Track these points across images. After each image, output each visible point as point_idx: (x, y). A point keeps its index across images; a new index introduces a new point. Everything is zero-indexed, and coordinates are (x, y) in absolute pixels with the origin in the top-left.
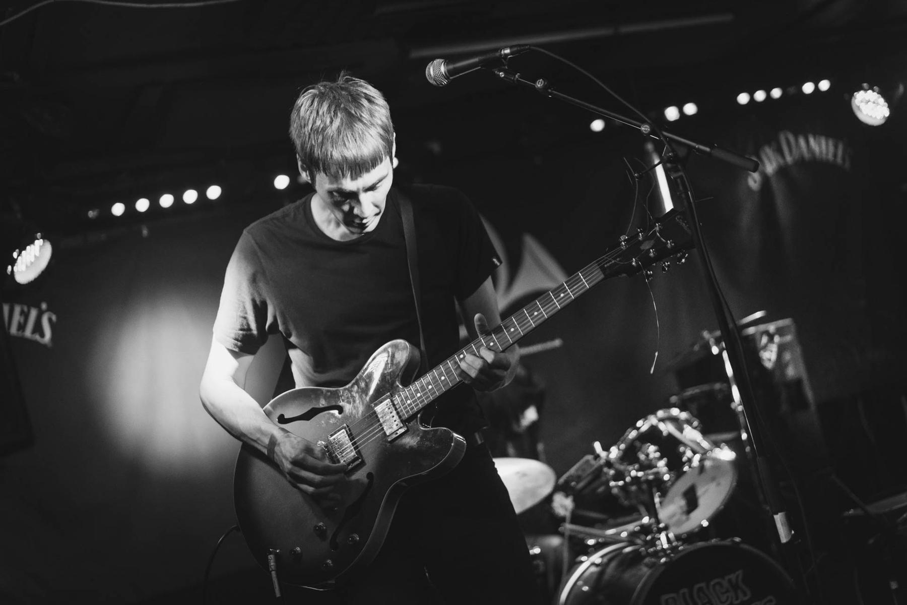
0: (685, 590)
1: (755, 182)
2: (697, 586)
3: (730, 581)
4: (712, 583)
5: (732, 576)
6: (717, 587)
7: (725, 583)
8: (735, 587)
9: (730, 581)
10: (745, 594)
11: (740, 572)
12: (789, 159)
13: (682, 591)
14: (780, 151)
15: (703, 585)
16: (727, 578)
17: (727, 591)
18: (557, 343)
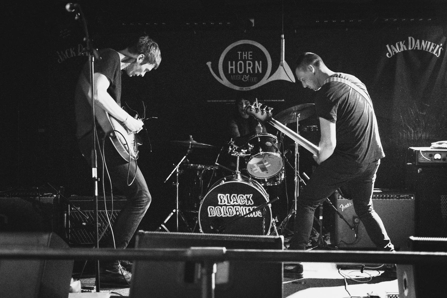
0: (229, 195)
1: (389, 55)
2: (233, 195)
3: (247, 197)
4: (239, 195)
5: (248, 196)
6: (241, 197)
7: (245, 197)
8: (248, 199)
9: (247, 197)
10: (251, 203)
11: (252, 195)
12: (410, 49)
13: (227, 195)
14: (406, 44)
15: (236, 195)
16: (246, 195)
17: (245, 200)
18: (283, 100)
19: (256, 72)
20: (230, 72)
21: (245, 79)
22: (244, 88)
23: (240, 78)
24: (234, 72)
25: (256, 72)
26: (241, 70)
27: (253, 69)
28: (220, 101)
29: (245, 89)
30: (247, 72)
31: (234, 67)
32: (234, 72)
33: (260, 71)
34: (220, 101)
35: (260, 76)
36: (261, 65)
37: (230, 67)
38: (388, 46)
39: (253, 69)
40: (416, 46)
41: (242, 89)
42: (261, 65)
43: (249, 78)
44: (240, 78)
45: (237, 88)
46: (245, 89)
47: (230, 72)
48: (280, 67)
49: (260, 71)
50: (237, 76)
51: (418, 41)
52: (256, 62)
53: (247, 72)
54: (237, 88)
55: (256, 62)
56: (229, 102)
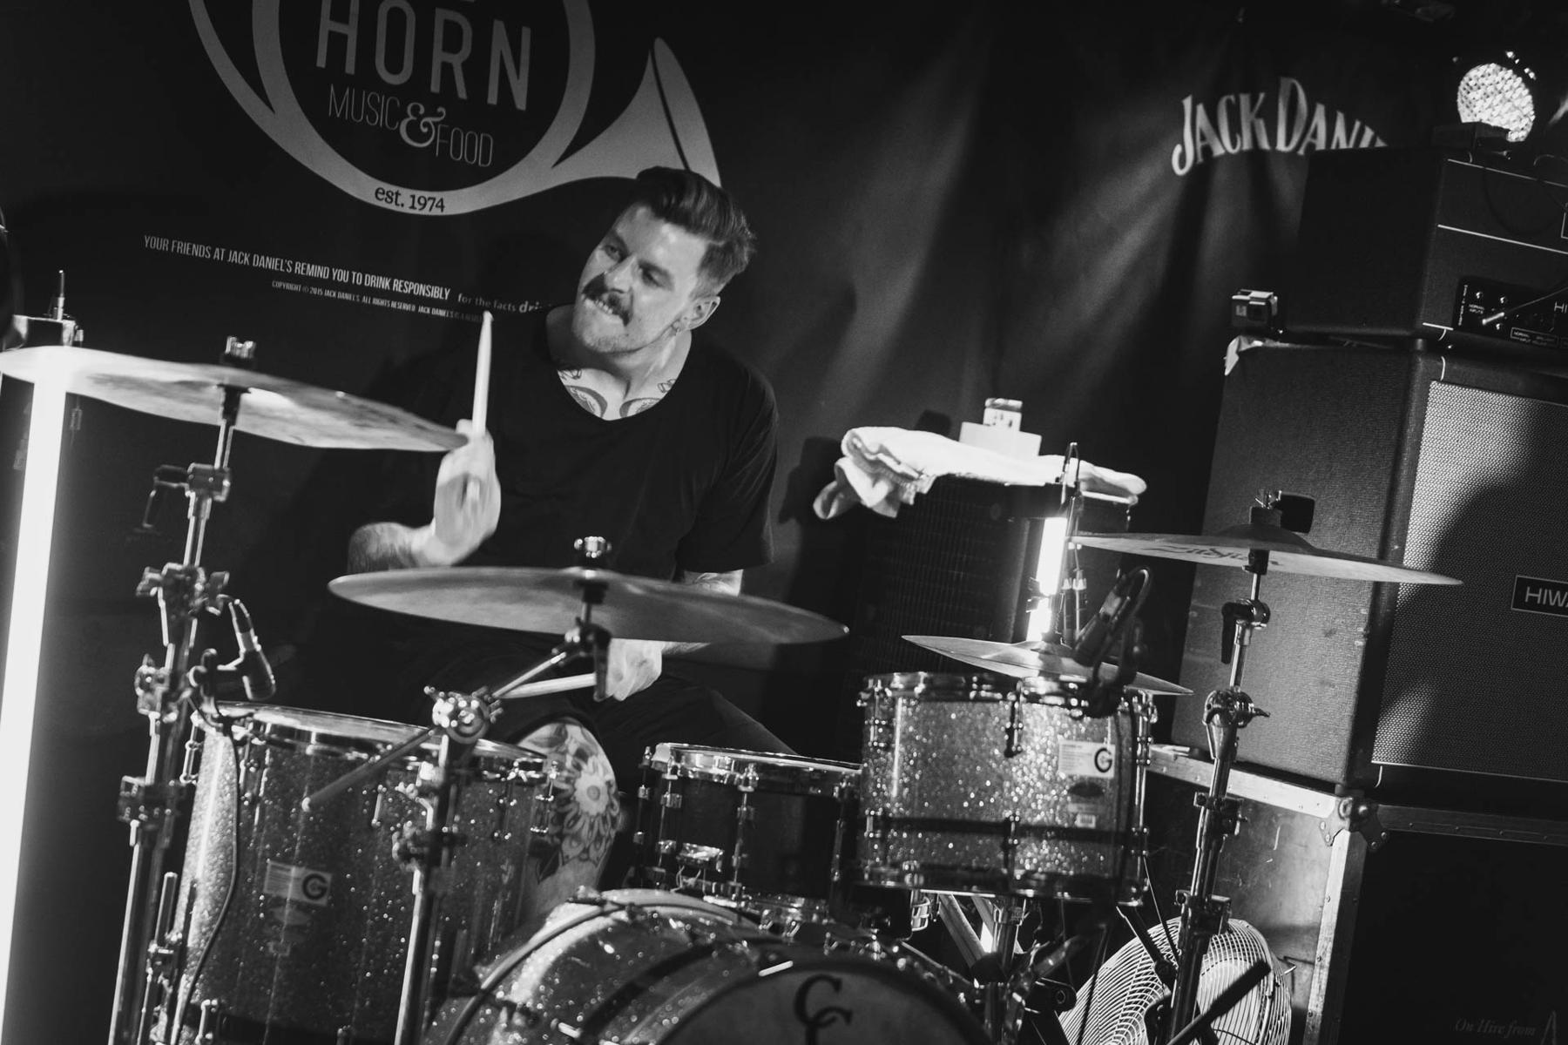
19: (492, 99)
20: (321, 62)
21: (413, 130)
22: (406, 195)
23: (381, 119)
24: (350, 68)
25: (492, 99)
26: (394, 66)
27: (477, 69)
28: (234, 257)
29: (407, 201)
30: (435, 87)
31: (351, 31)
32: (350, 68)
33: (521, 104)
34: (234, 257)
35: (514, 139)
36: (525, 57)
37: (327, 25)
38: (1187, 103)
39: (477, 69)
40: (1308, 139)
41: (391, 197)
42: (525, 57)
43: (445, 134)
44: (381, 119)
45: (361, 186)
46: (407, 201)
47: (321, 62)
48: (644, 100)
49: (521, 104)
50: (366, 99)
51: (1320, 110)
52: (499, 30)
53: (435, 87)
54: (361, 186)
55: (499, 30)
56: (294, 278)
